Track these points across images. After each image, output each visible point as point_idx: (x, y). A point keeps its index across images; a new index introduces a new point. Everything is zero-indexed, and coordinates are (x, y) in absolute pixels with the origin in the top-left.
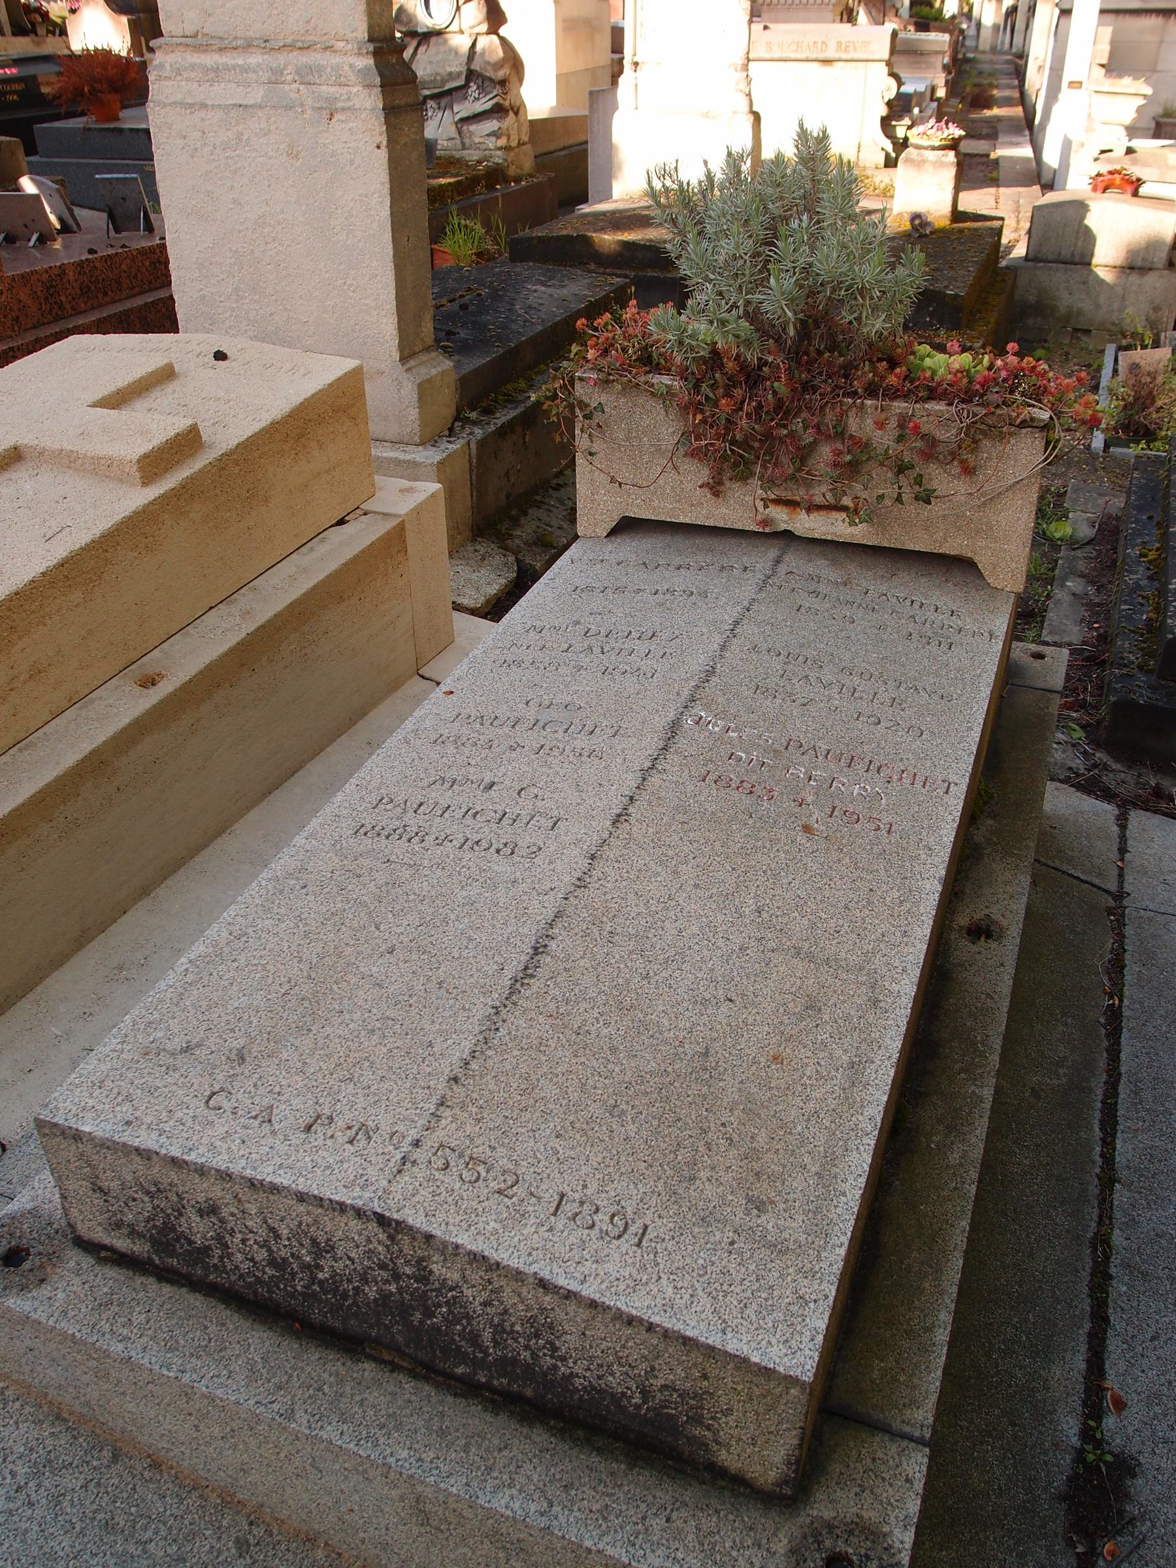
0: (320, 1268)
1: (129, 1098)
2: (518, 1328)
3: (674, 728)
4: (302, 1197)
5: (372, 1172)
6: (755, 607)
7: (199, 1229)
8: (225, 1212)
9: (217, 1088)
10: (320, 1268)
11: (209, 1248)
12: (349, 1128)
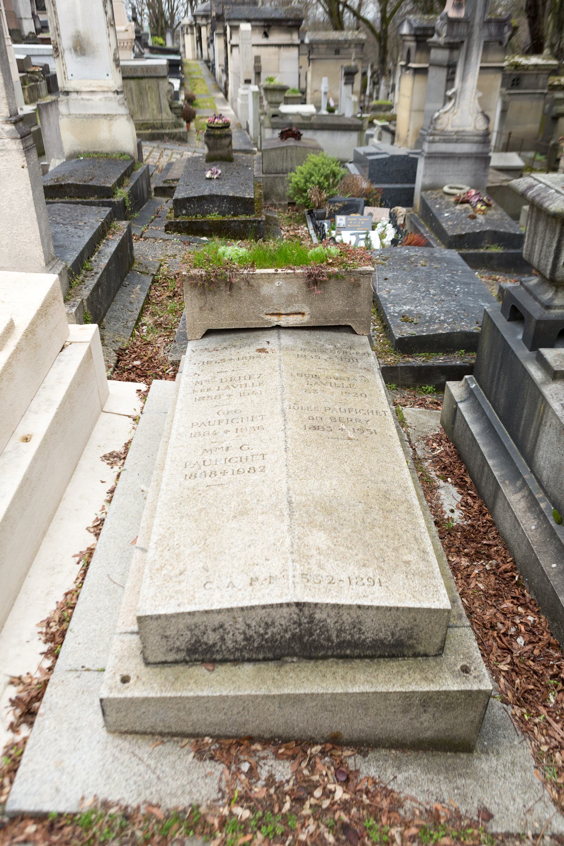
0: (266, 633)
1: (171, 597)
2: (347, 628)
3: (283, 410)
4: (264, 607)
5: (286, 591)
6: (282, 358)
7: (212, 638)
8: (227, 626)
9: (205, 582)
10: (266, 633)
11: (216, 643)
12: (266, 579)
